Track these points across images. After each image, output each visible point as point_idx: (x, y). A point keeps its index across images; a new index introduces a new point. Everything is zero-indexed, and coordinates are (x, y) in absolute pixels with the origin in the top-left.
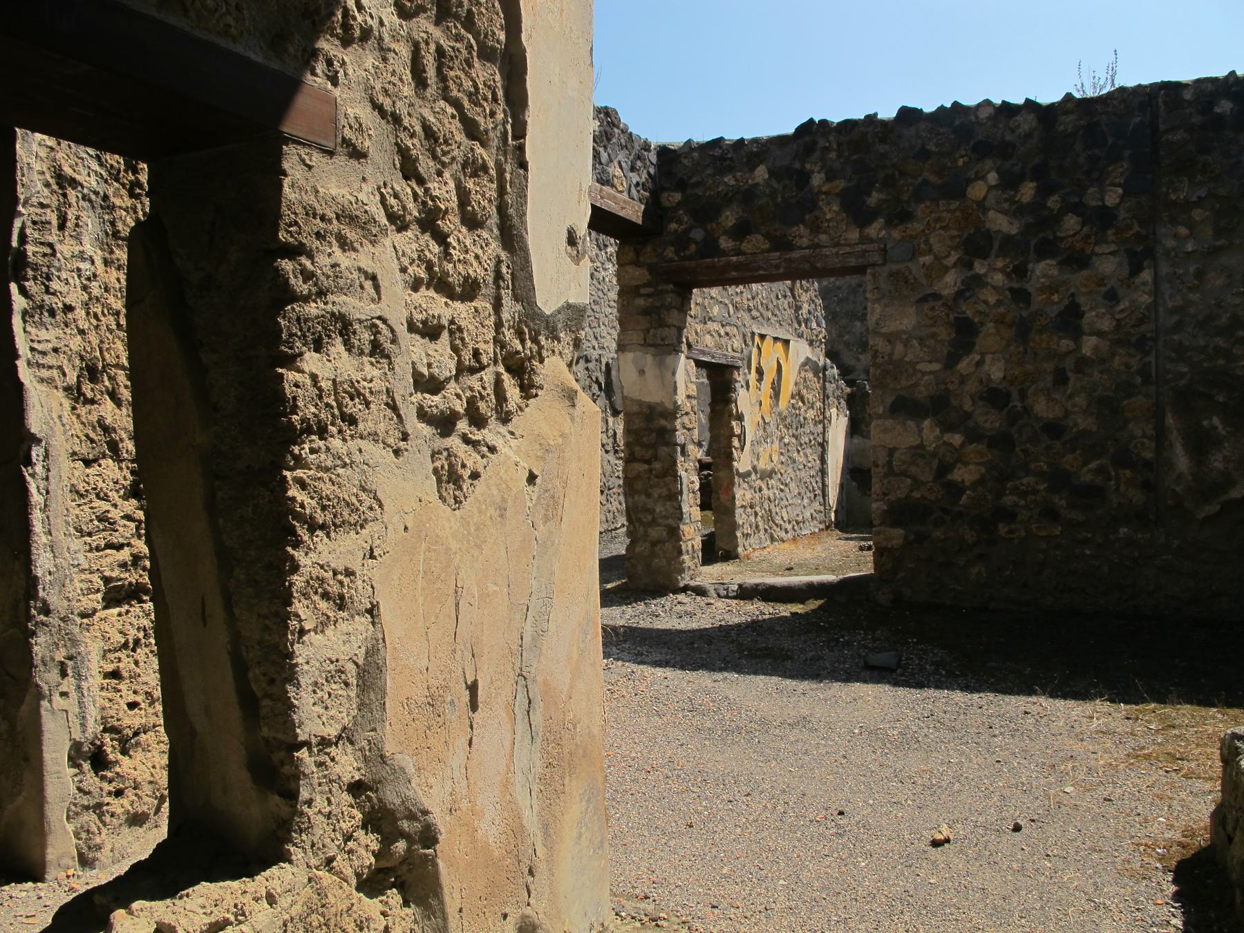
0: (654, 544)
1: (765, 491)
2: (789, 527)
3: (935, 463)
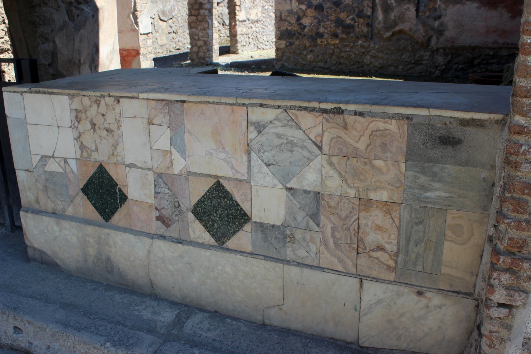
0: (199, 47)
1: (254, 29)
2: (267, 44)
3: (296, 16)
